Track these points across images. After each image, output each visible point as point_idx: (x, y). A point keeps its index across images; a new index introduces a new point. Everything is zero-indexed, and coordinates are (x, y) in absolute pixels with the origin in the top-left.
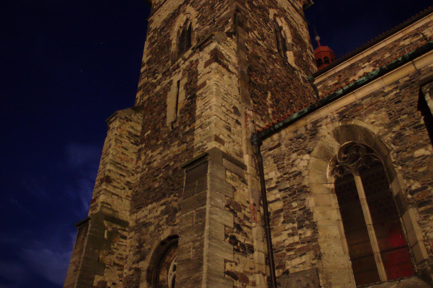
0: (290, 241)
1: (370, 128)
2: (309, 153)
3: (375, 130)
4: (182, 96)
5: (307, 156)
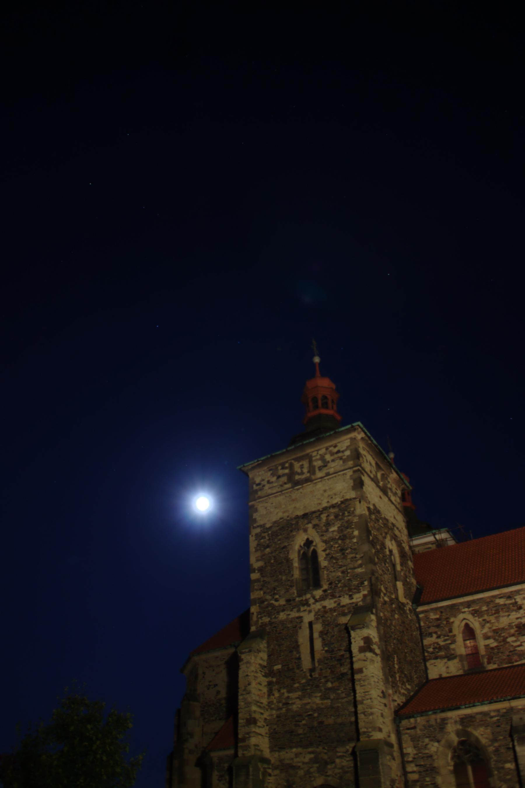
1: (480, 737)
2: (438, 741)
3: (484, 741)
4: (318, 644)
5: (436, 744)
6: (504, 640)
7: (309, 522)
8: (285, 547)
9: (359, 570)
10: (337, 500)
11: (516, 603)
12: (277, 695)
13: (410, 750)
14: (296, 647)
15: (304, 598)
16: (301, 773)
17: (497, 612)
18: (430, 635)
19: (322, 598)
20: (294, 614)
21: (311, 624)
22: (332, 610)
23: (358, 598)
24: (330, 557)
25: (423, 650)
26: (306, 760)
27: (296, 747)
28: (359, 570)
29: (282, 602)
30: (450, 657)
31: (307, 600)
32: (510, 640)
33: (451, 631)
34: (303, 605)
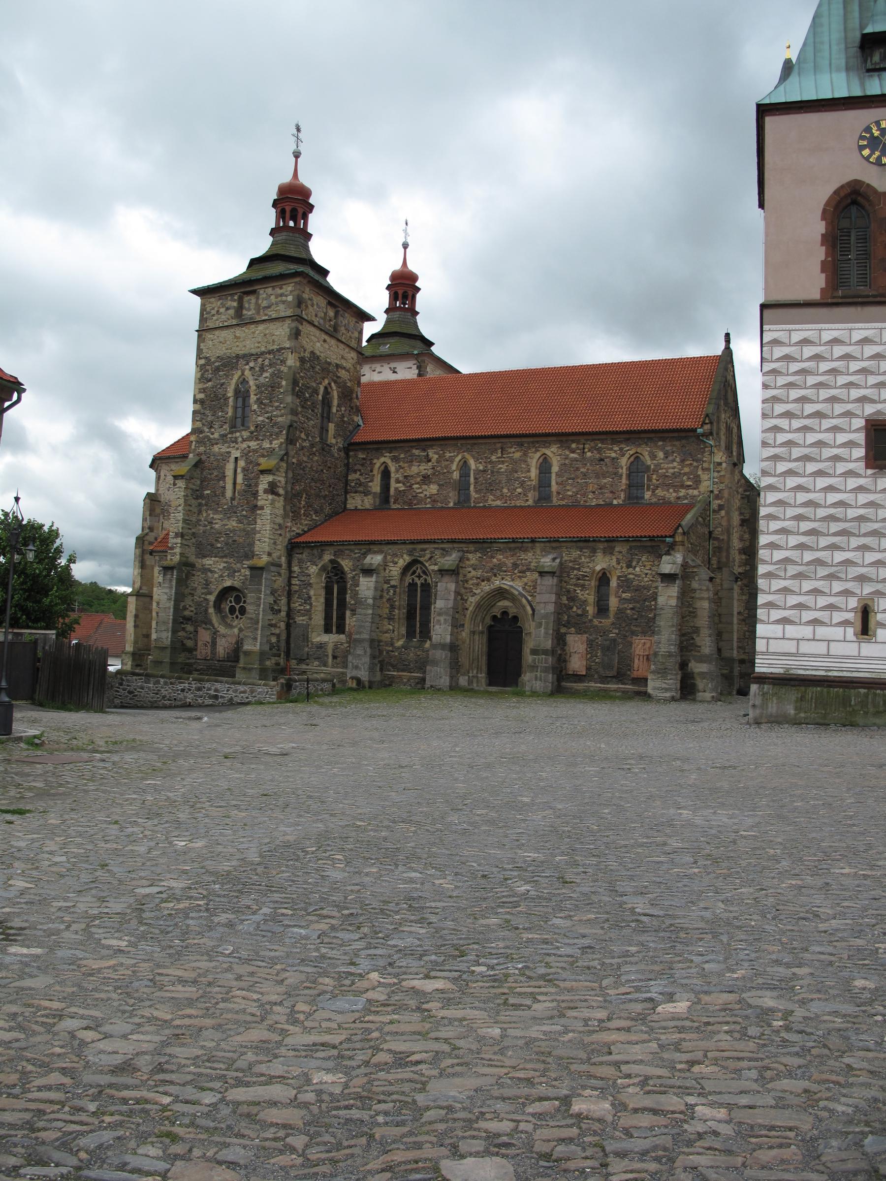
0: (299, 608)
3: (346, 569)
5: (315, 567)
6: (410, 486)
7: (247, 364)
8: (222, 385)
9: (280, 419)
10: (275, 347)
11: (428, 455)
12: (205, 515)
13: (296, 569)
14: (224, 477)
15: (234, 435)
16: (216, 576)
17: (412, 461)
18: (355, 472)
19: (249, 439)
20: (224, 449)
21: (236, 458)
22: (255, 451)
23: (276, 444)
24: (259, 402)
25: (347, 483)
26: (221, 567)
27: (215, 557)
28: (280, 419)
29: (216, 436)
30: (366, 493)
31: (236, 438)
32: (415, 486)
33: (372, 471)
34: (233, 442)
